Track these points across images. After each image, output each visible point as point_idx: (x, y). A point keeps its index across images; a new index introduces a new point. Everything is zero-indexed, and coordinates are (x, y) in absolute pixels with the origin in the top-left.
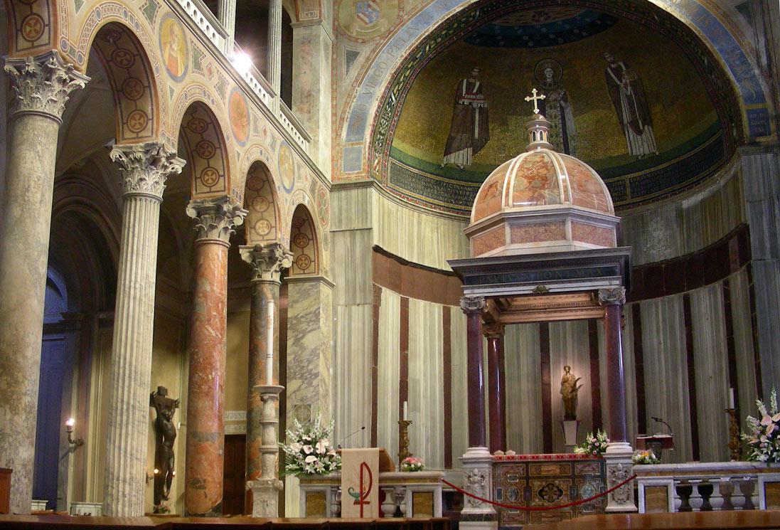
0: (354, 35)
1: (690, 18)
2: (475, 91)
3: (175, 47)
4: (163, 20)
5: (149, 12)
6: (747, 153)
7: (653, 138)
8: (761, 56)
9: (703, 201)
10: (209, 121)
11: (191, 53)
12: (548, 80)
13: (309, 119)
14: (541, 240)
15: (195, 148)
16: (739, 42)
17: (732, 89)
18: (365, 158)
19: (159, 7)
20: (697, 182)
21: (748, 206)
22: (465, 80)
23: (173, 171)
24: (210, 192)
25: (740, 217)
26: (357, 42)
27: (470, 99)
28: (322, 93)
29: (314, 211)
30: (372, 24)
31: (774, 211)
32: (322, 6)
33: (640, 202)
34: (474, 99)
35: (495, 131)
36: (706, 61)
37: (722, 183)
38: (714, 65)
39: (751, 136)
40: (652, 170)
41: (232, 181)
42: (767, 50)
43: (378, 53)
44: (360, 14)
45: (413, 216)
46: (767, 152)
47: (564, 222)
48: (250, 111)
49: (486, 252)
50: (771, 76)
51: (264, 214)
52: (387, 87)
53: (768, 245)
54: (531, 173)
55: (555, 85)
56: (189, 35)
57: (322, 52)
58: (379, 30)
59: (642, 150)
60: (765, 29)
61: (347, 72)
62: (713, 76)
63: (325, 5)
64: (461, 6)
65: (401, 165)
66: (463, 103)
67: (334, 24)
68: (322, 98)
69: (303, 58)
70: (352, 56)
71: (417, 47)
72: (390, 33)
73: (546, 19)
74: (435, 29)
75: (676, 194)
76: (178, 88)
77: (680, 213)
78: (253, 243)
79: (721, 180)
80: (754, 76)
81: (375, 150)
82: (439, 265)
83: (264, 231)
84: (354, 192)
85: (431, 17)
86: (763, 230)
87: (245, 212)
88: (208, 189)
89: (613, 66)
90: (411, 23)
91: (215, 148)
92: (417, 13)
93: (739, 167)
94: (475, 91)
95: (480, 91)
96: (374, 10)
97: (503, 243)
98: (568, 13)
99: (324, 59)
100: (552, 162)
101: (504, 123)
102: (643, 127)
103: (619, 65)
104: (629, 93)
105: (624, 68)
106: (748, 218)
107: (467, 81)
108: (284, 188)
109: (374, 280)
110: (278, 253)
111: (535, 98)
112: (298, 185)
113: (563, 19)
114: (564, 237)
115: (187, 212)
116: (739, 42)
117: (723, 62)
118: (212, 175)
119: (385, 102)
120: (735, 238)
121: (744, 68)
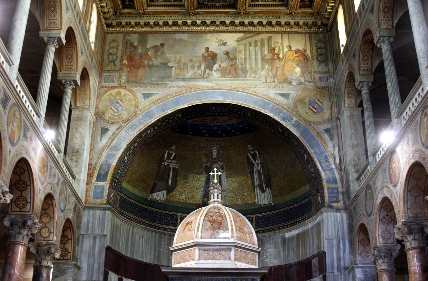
0: (107, 118)
1: (299, 133)
2: (172, 158)
3: (15, 124)
4: (11, 108)
5: (4, 103)
6: (326, 212)
7: (271, 195)
8: (336, 158)
9: (298, 235)
10: (26, 169)
11: (23, 128)
12: (214, 156)
13: (76, 166)
14: (216, 259)
15: (14, 184)
16: (325, 149)
17: (320, 175)
18: (106, 193)
19: (10, 100)
20: (295, 224)
21: (326, 242)
22: (167, 152)
23: (5, 201)
24: (20, 211)
25: (320, 247)
26: (108, 123)
27: (169, 162)
28: (85, 151)
29: (74, 222)
30: (118, 114)
31: (340, 245)
32: (91, 100)
33: (261, 231)
34: (170, 163)
35: (181, 181)
36: (306, 157)
37: (310, 226)
38: (311, 160)
39: (329, 202)
40: (269, 213)
41: (35, 206)
42: (339, 155)
43: (121, 131)
44: (112, 107)
45: (129, 228)
46: (337, 212)
47: (230, 250)
48: (49, 163)
49: (182, 263)
50: (341, 170)
51: (47, 224)
52: (123, 152)
53: (336, 264)
54: (213, 219)
55: (217, 159)
56: (23, 117)
57: (88, 127)
58: (122, 118)
60: (339, 144)
61: (101, 139)
62: (309, 166)
63: (93, 99)
64: (171, 110)
65: (126, 197)
66: (164, 164)
67: (96, 110)
68: (85, 154)
69: (76, 129)
70: (105, 131)
71: (143, 131)
72: (128, 120)
73: (217, 123)
74: (155, 122)
75: (282, 229)
76: (13, 150)
77: (284, 240)
78: (38, 241)
79: (309, 224)
80: (332, 169)
81: (112, 188)
82: (142, 259)
83: (46, 235)
84: (98, 212)
85: (154, 114)
86: (333, 256)
87: (40, 225)
88: (19, 210)
89: (252, 152)
90: (142, 116)
91: (27, 185)
92: (145, 111)
93: (321, 219)
94: (172, 158)
95: (174, 158)
96: (120, 105)
97: (194, 260)
98: (231, 121)
99: (88, 131)
100: (225, 213)
101: (186, 178)
103: (256, 153)
104: (259, 169)
105: (258, 154)
106: (326, 248)
107: (168, 152)
108: (61, 209)
109: (105, 267)
110: (53, 250)
111: (215, 173)
112: (68, 207)
113: (228, 123)
114: (230, 259)
115: (4, 222)
116: (325, 149)
117: (316, 159)
118: (23, 201)
119: (121, 159)
120: (317, 258)
121: (327, 164)
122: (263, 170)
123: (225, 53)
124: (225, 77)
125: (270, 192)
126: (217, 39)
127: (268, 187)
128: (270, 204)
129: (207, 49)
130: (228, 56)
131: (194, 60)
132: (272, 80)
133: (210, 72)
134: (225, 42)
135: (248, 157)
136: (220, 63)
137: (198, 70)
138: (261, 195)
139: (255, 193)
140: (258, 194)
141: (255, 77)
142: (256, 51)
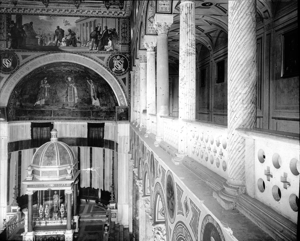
2: (45, 83)
22: (42, 81)
94: (45, 83)
123: (69, 30)
124: (69, 46)
126: (64, 21)
129: (58, 27)
130: (71, 33)
131: (50, 34)
132: (95, 48)
133: (60, 42)
134: (69, 22)
136: (66, 37)
137: (53, 41)
141: (85, 46)
142: (87, 30)
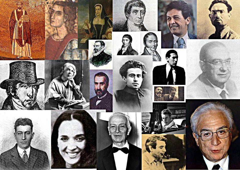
7: (30, 50)
59: (21, 54)
89: (19, 10)
102: (25, 44)
103: (22, 12)
104: (20, 27)
105: (24, 14)
122: (24, 28)
125: (30, 48)
127: (28, 43)
128: (28, 57)
135: (13, 13)
138: (18, 47)
139: (12, 45)
140: (16, 46)
